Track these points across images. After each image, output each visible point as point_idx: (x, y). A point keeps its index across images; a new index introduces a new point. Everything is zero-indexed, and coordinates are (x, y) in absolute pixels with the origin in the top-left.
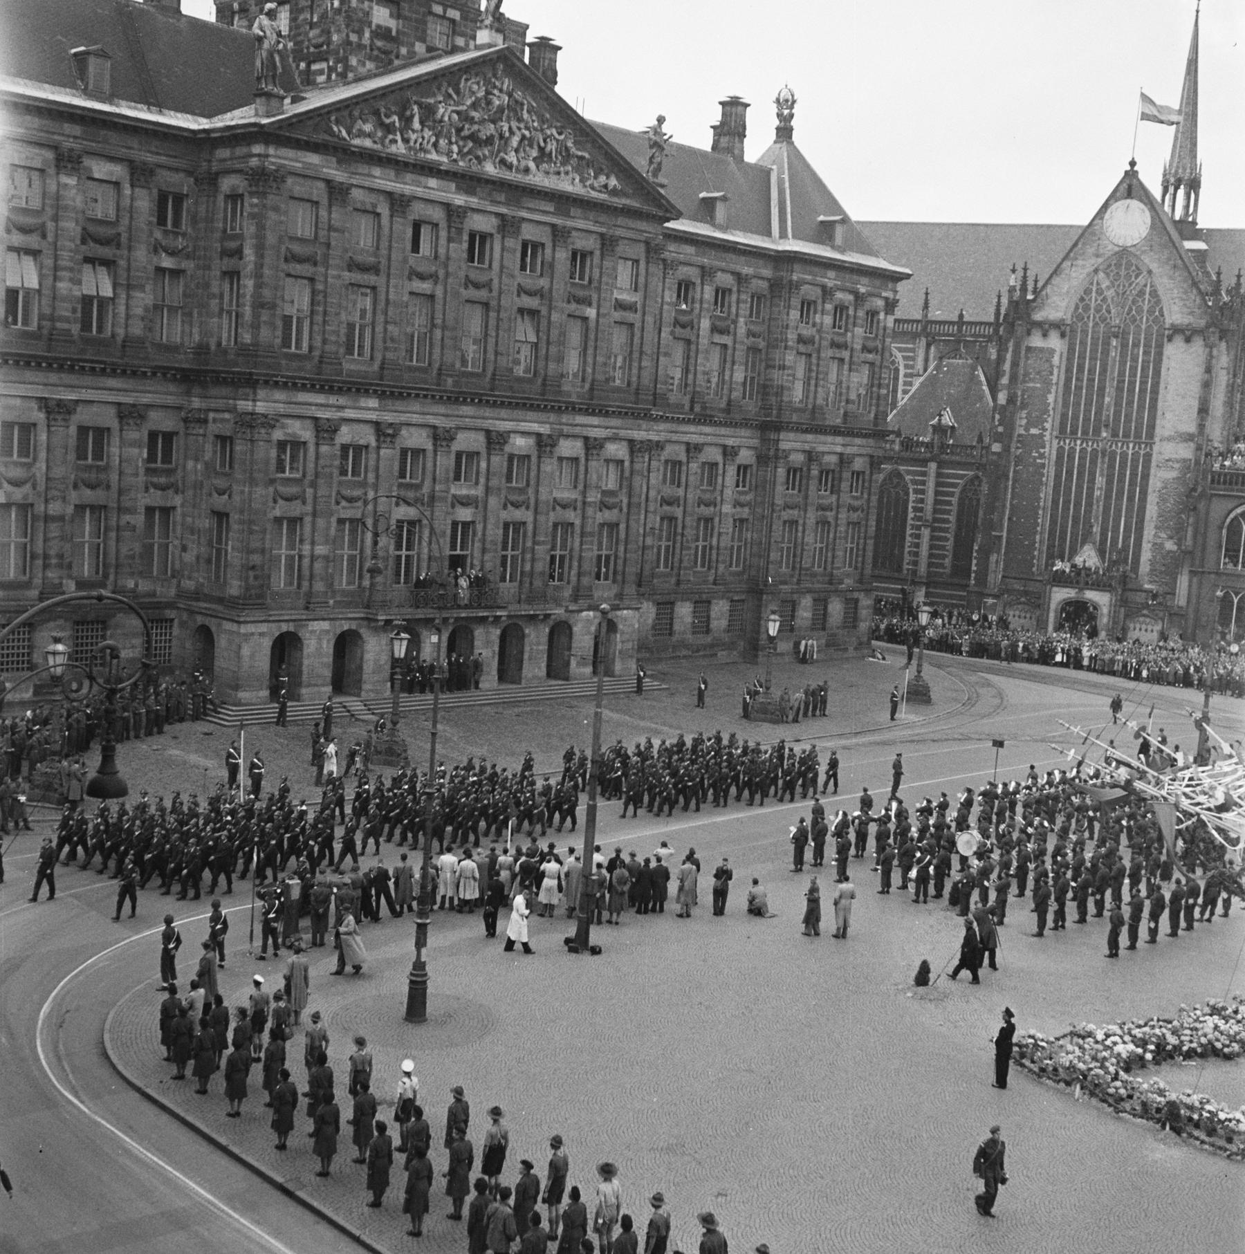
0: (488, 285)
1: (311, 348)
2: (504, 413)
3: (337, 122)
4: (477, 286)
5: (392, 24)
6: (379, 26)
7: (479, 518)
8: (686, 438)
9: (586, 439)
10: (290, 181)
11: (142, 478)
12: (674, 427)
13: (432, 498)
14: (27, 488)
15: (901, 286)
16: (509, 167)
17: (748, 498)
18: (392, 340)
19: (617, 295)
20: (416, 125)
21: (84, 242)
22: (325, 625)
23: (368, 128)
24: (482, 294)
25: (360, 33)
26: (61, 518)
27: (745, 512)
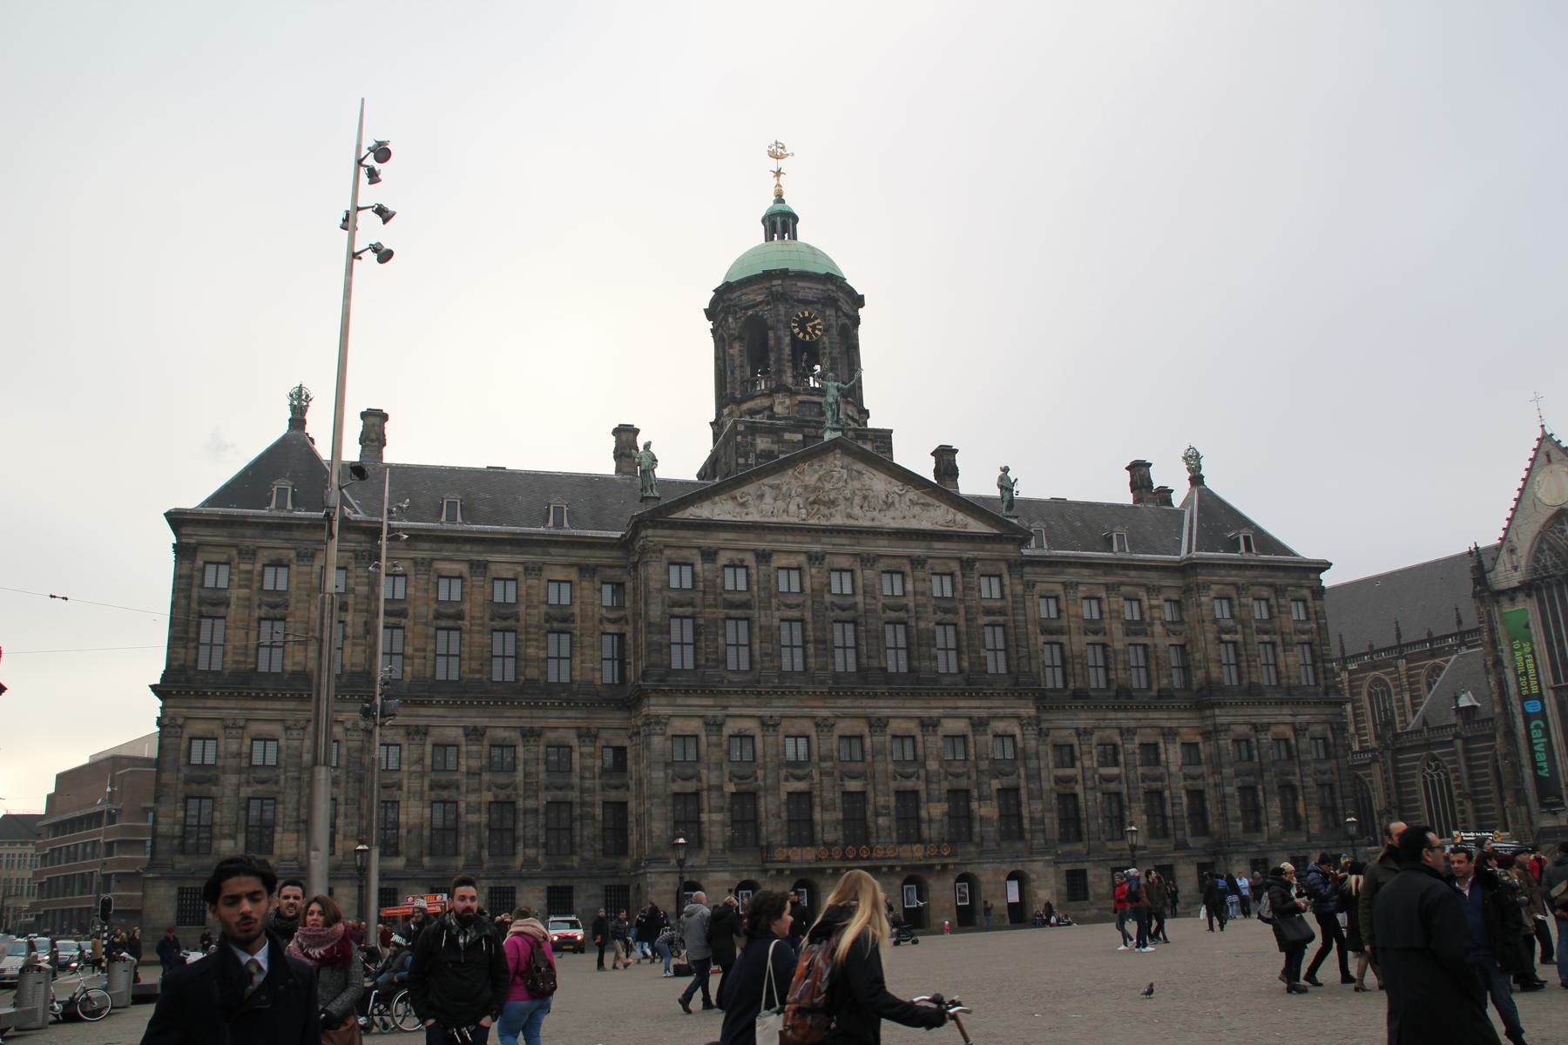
0: (854, 606)
1: (697, 666)
2: (881, 703)
7: (870, 788)
9: (970, 718)
10: (668, 552)
12: (1101, 715)
14: (509, 791)
15: (1322, 576)
17: (1197, 770)
18: (767, 655)
20: (768, 499)
21: (547, 621)
22: (726, 876)
25: (746, 457)
27: (1199, 784)
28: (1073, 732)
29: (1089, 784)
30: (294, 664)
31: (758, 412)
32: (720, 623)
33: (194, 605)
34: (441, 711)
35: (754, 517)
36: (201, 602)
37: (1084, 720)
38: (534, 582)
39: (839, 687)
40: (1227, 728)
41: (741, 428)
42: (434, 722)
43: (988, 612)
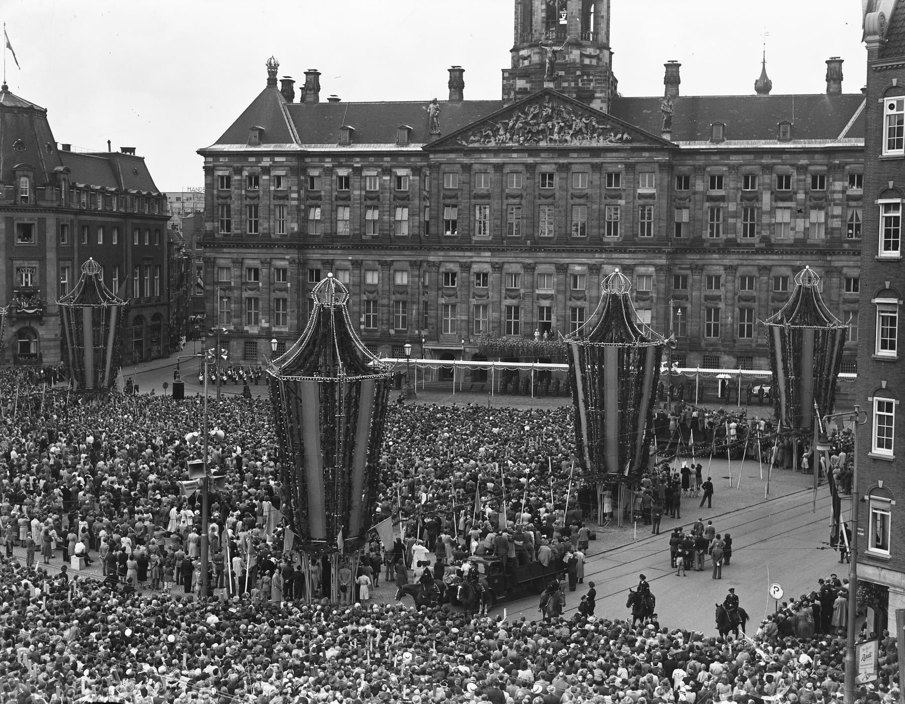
2: (564, 255)
3: (462, 138)
4: (547, 197)
5: (528, 86)
6: (520, 89)
8: (757, 262)
10: (443, 166)
11: (421, 290)
12: (745, 257)
13: (524, 294)
16: (555, 141)
18: (497, 226)
19: (639, 191)
20: (501, 132)
21: (394, 200)
23: (476, 138)
24: (550, 201)
25: (509, 94)
26: (388, 306)
28: (722, 268)
29: (730, 302)
30: (264, 229)
31: (525, 58)
32: (472, 208)
33: (215, 199)
34: (339, 252)
35: (493, 144)
36: (218, 197)
37: (731, 260)
38: (388, 178)
39: (538, 245)
40: (839, 270)
41: (506, 75)
42: (336, 257)
43: (641, 196)
